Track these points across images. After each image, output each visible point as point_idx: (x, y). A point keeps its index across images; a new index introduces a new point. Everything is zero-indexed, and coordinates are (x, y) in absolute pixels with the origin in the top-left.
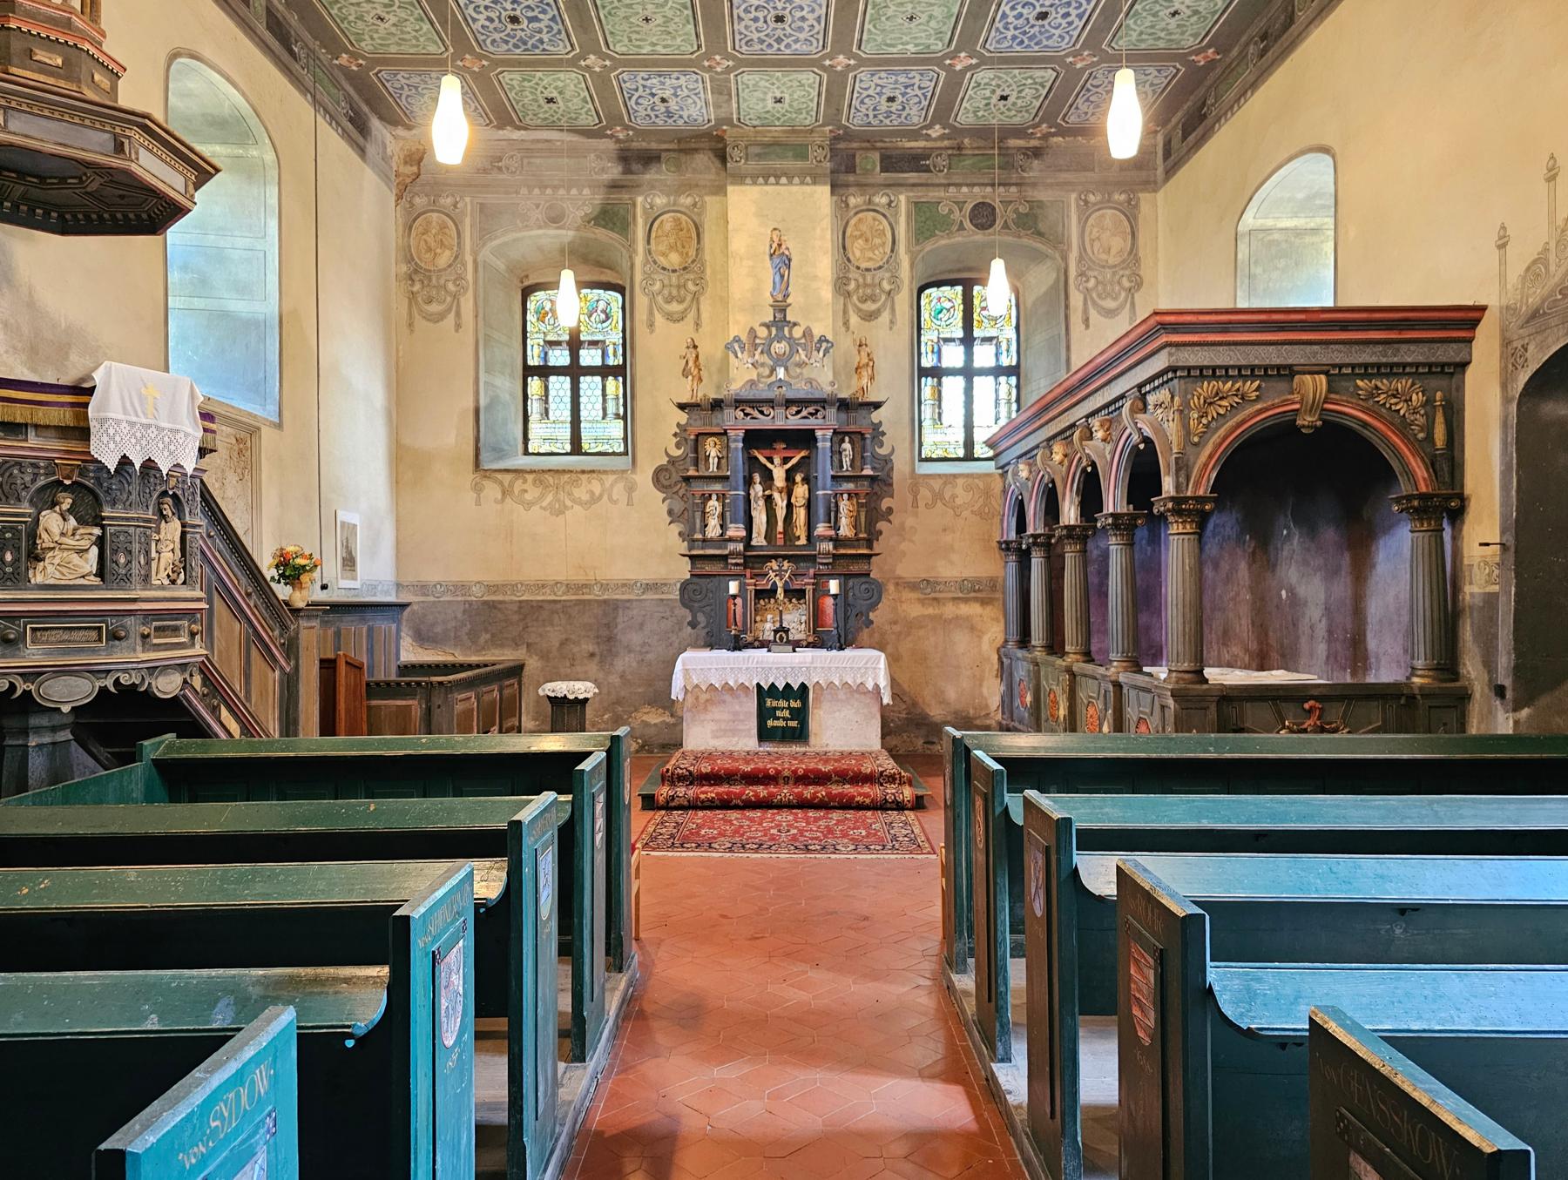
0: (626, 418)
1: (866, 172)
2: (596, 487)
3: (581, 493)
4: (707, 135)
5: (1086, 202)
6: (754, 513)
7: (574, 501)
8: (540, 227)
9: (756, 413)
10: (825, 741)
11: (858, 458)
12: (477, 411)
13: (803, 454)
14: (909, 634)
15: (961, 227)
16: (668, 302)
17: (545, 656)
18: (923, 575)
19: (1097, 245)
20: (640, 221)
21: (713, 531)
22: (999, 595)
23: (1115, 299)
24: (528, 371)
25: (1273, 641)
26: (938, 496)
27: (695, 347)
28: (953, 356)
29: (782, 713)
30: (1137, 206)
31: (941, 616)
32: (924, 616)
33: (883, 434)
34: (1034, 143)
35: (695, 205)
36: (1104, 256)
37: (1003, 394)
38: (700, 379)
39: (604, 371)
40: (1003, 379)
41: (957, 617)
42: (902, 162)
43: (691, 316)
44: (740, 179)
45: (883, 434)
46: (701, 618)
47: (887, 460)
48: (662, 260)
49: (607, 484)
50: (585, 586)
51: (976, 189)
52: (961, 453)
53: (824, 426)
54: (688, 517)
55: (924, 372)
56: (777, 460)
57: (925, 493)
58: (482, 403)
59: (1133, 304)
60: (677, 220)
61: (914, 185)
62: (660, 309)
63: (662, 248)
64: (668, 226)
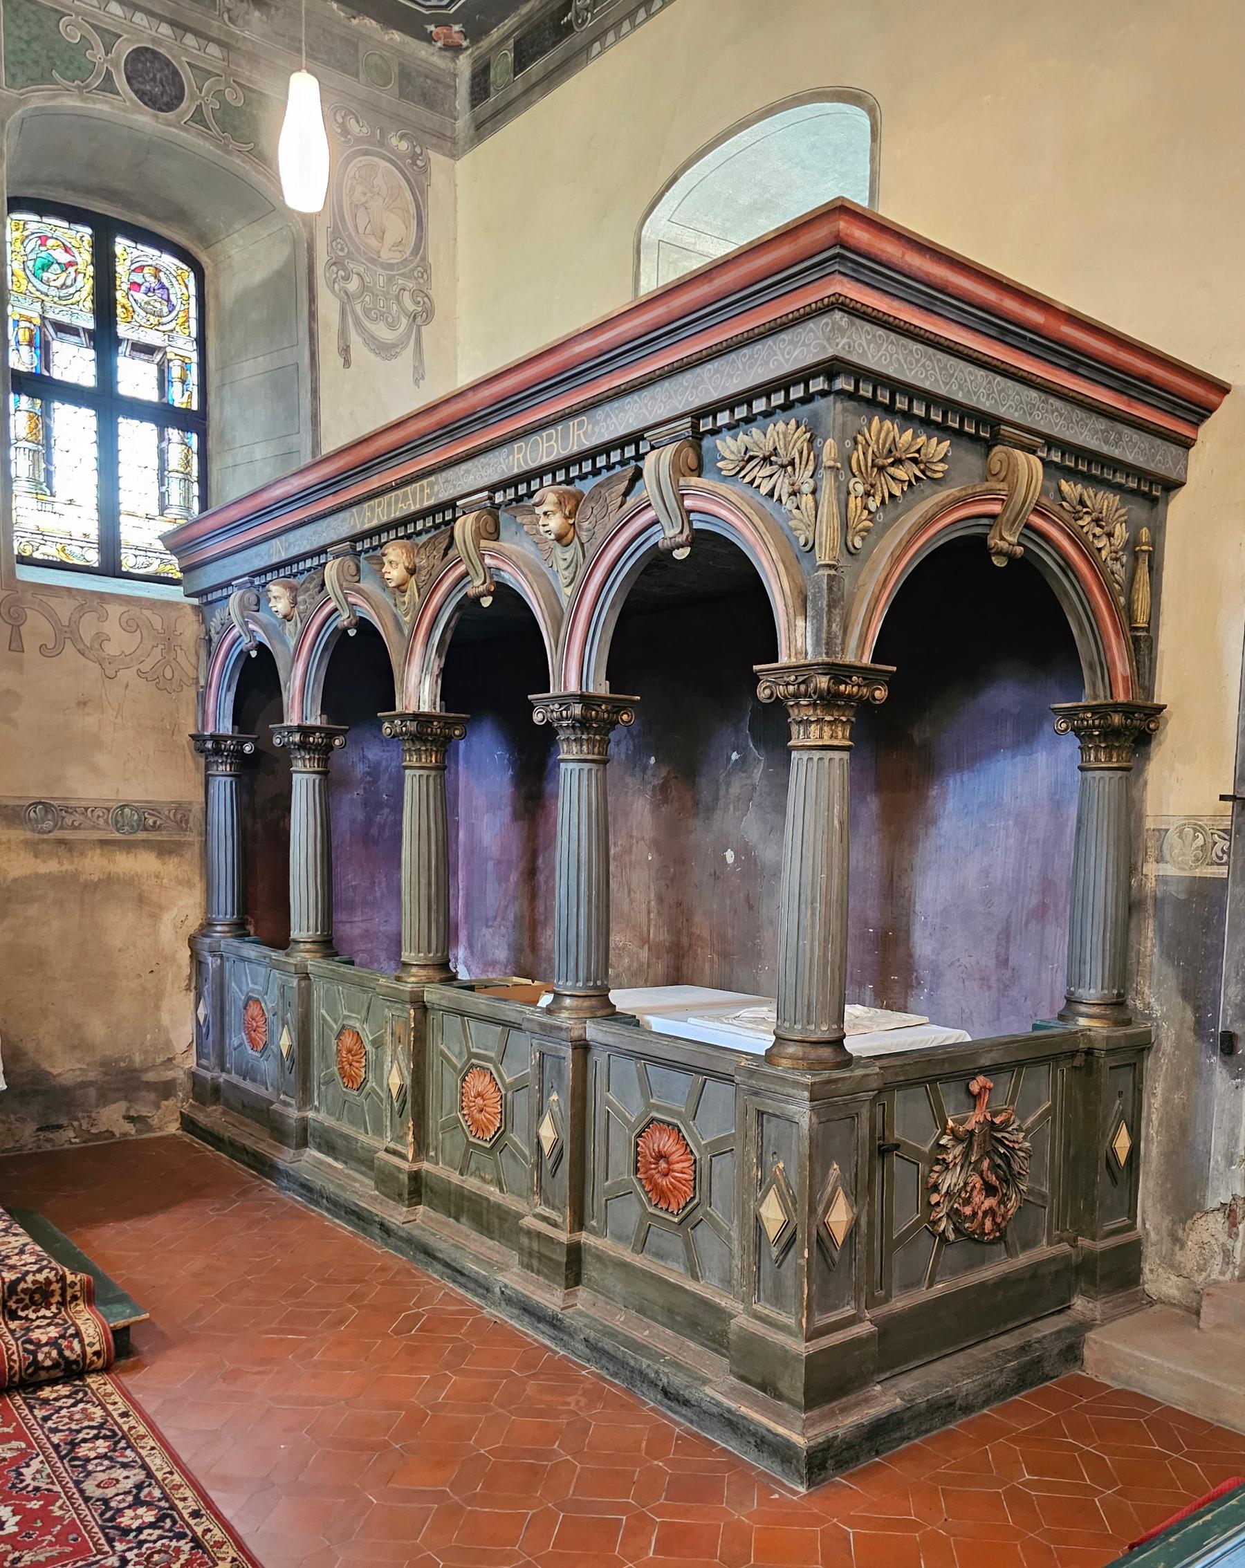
18: (38, 794)
22: (193, 837)
23: (391, 326)
25: (702, 926)
31: (75, 876)
36: (373, 242)
37: (175, 455)
40: (174, 434)
41: (109, 880)
51: (139, 18)
52: (93, 558)
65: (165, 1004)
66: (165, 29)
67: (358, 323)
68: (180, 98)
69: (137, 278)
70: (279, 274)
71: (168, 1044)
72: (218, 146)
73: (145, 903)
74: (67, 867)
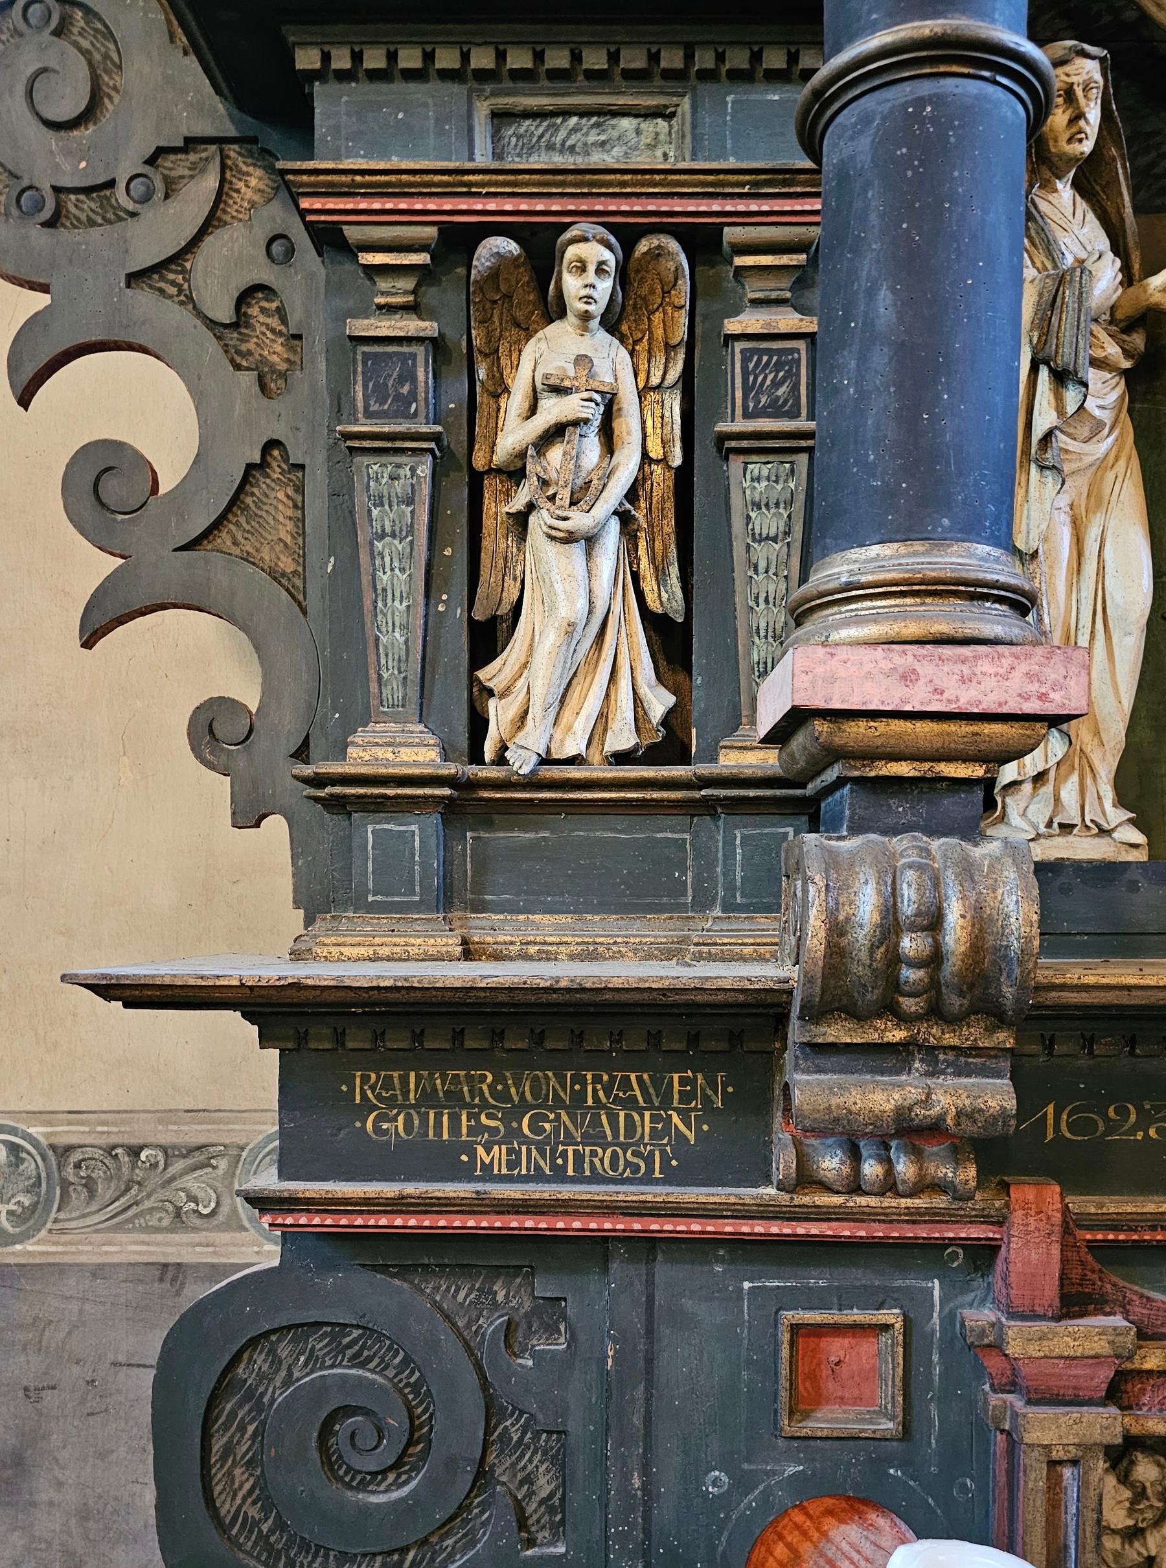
21: (570, 681)
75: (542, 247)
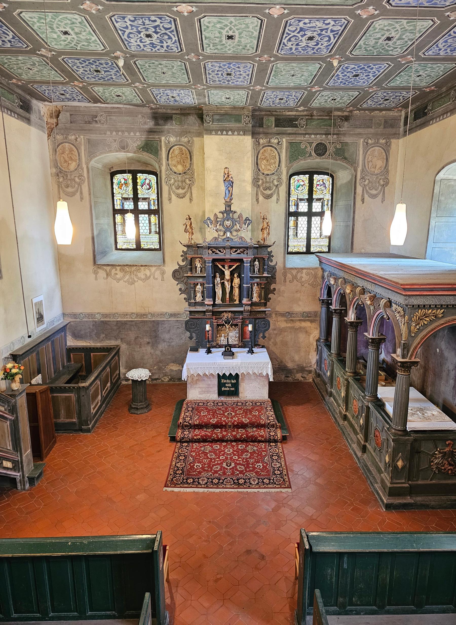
0: (160, 233)
1: (268, 127)
2: (148, 272)
3: (141, 275)
4: (195, 108)
5: (367, 143)
6: (216, 290)
7: (138, 279)
8: (117, 151)
9: (218, 252)
10: (245, 395)
11: (261, 268)
12: (93, 238)
13: (237, 264)
14: (280, 334)
15: (310, 155)
16: (178, 189)
17: (129, 343)
19: (370, 164)
20: (163, 149)
22: (318, 319)
23: (376, 190)
24: (115, 212)
26: (295, 277)
27: (190, 219)
28: (304, 207)
29: (229, 385)
30: (390, 146)
32: (287, 327)
33: (273, 256)
34: (346, 114)
35: (189, 142)
36: (373, 170)
38: (193, 234)
39: (149, 212)
41: (300, 328)
42: (285, 121)
43: (188, 195)
44: (209, 131)
45: (273, 256)
46: (194, 335)
47: (274, 268)
48: (174, 169)
49: (153, 271)
50: (145, 315)
51: (318, 136)
53: (247, 258)
54: (188, 292)
55: (290, 214)
56: (226, 268)
57: (289, 276)
58: (95, 233)
59: (384, 192)
60: (181, 150)
61: (290, 134)
62: (174, 192)
63: (174, 162)
64: (177, 152)
65: (310, 354)
66: (324, 136)
67: (367, 191)
68: (326, 152)
69: (318, 183)
70: (349, 182)
71: (311, 362)
72: (334, 160)
73: (307, 333)
74: (292, 325)
75: (198, 284)
